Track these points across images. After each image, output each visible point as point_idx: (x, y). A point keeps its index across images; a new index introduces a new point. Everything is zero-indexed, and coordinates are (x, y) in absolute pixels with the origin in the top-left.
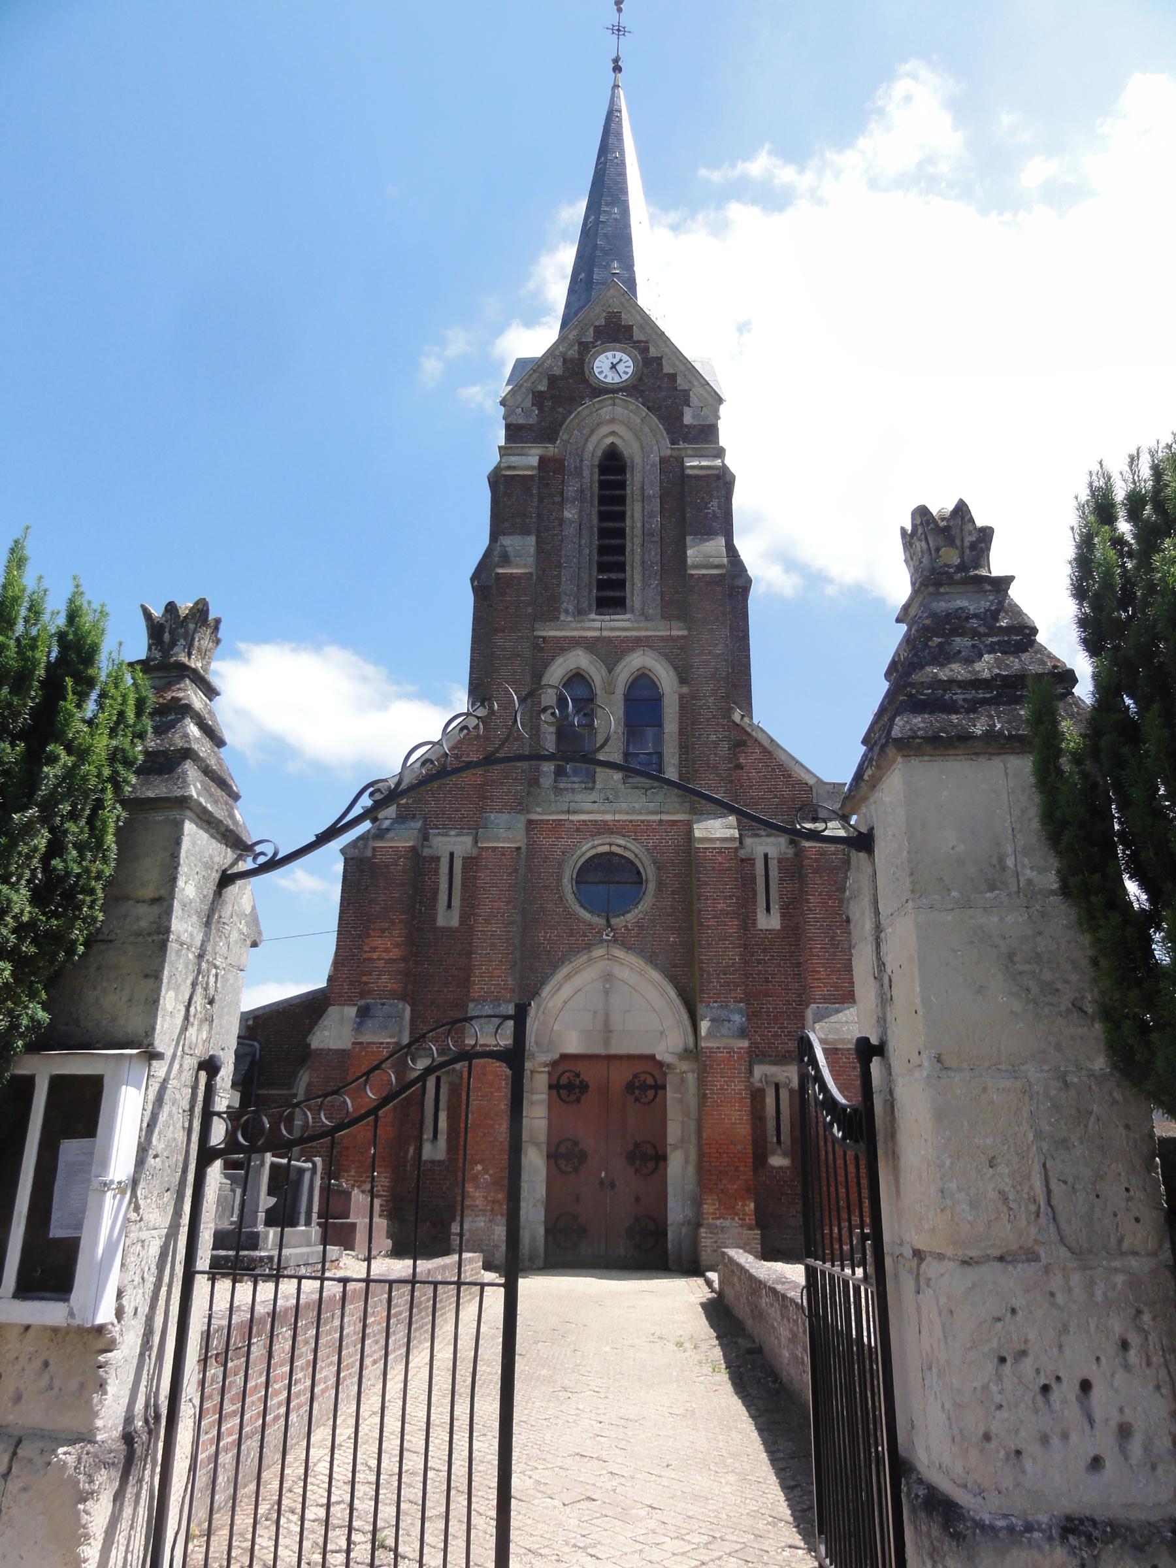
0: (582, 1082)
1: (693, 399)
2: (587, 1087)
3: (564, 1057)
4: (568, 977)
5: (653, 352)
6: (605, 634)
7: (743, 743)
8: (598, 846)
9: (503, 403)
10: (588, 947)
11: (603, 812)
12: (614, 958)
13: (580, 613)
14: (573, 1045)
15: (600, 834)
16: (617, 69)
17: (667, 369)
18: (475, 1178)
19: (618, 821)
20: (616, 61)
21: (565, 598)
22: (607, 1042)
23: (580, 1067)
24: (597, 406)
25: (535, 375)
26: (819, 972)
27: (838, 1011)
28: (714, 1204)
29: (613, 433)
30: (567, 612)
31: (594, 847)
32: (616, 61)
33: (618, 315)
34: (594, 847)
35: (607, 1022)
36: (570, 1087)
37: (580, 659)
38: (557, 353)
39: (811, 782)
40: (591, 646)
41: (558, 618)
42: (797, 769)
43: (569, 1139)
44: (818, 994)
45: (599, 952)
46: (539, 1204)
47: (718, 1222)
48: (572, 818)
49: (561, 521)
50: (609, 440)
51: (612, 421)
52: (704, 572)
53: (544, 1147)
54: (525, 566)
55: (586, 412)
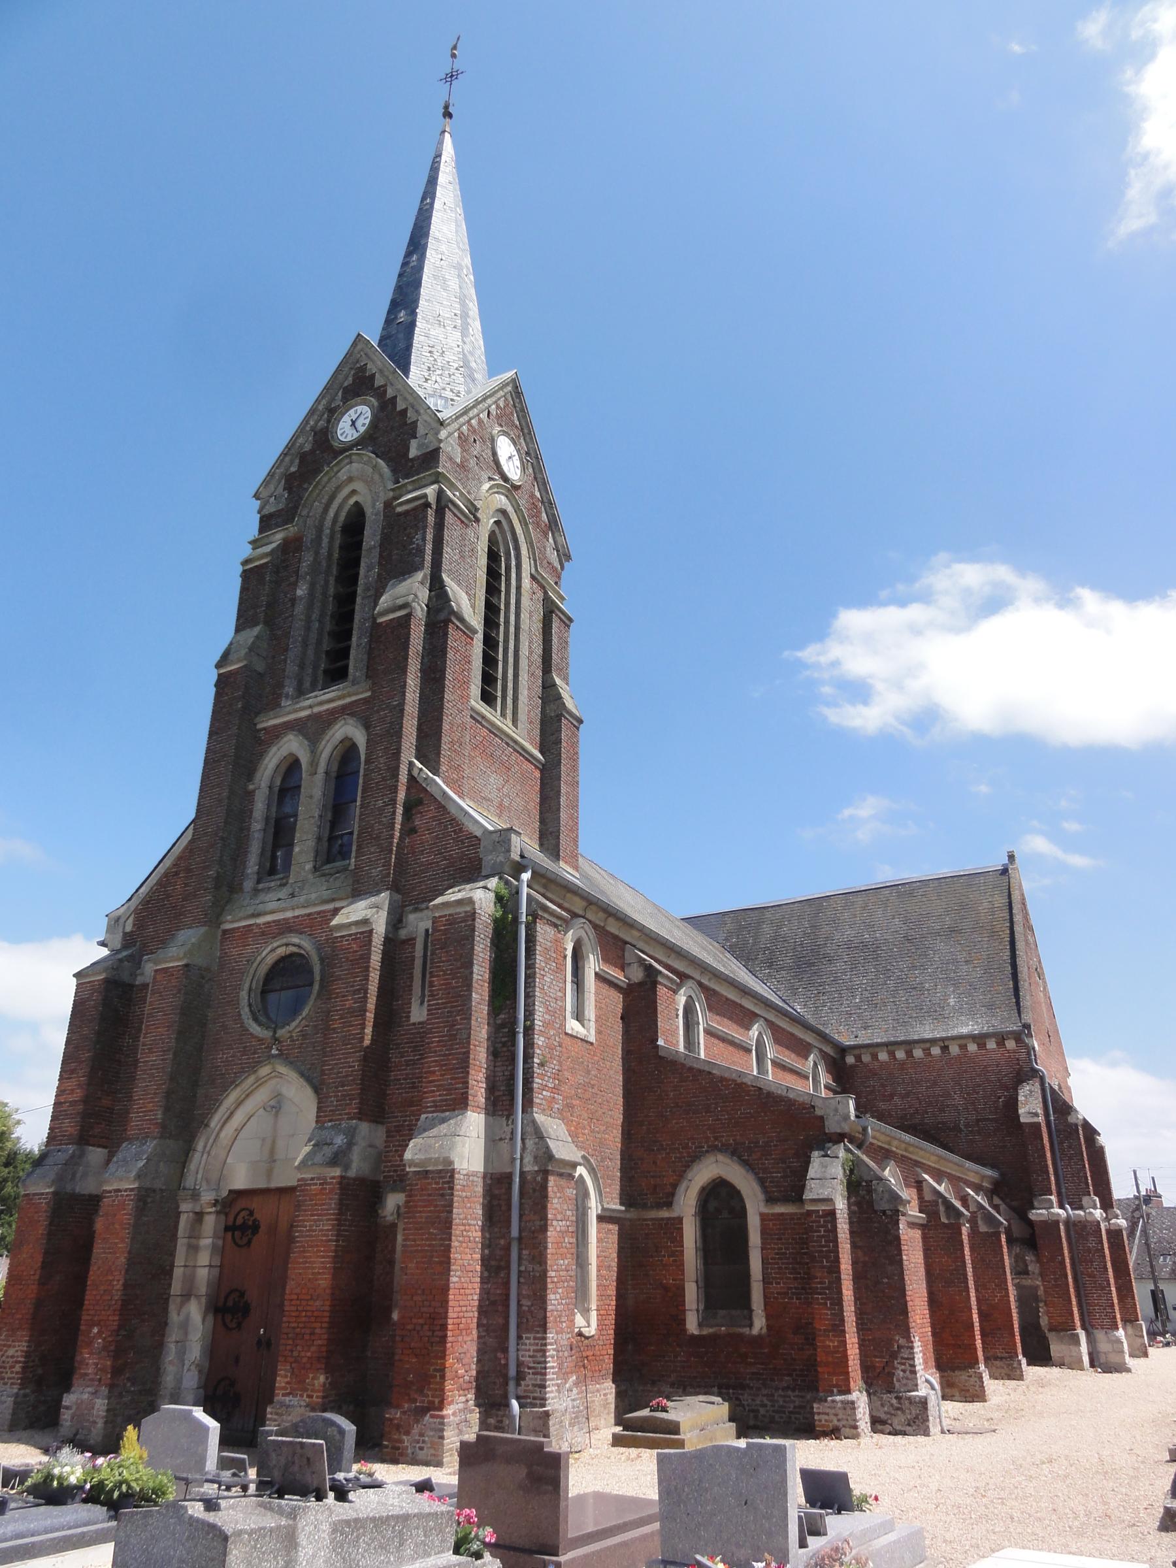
0: (255, 1220)
1: (421, 430)
2: (255, 1228)
3: (237, 1194)
4: (239, 1104)
5: (390, 393)
6: (316, 710)
7: (420, 802)
8: (271, 952)
9: (257, 496)
10: (253, 1067)
11: (283, 910)
12: (280, 1075)
13: (301, 693)
14: (240, 1180)
15: (282, 933)
16: (447, 114)
17: (400, 406)
18: (90, 1344)
19: (298, 917)
20: (446, 107)
21: (287, 682)
22: (269, 1174)
23: (255, 1203)
24: (335, 469)
25: (287, 459)
26: (434, 1072)
27: (443, 1121)
28: (286, 1376)
29: (354, 492)
30: (287, 696)
31: (273, 950)
32: (446, 107)
33: (363, 369)
34: (273, 950)
35: (272, 1152)
36: (243, 1228)
37: (292, 745)
38: (308, 428)
39: (478, 833)
40: (298, 727)
41: (279, 705)
42: (465, 821)
43: (236, 1290)
44: (429, 1100)
45: (264, 1071)
46: (193, 1368)
47: (287, 1399)
48: (260, 920)
49: (293, 601)
50: (352, 501)
51: (350, 480)
52: (391, 616)
53: (203, 1300)
54: (239, 661)
55: (325, 479)
